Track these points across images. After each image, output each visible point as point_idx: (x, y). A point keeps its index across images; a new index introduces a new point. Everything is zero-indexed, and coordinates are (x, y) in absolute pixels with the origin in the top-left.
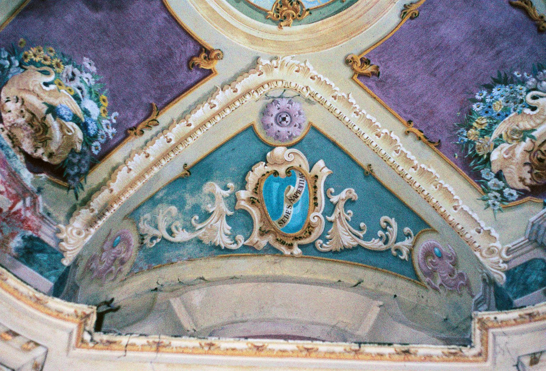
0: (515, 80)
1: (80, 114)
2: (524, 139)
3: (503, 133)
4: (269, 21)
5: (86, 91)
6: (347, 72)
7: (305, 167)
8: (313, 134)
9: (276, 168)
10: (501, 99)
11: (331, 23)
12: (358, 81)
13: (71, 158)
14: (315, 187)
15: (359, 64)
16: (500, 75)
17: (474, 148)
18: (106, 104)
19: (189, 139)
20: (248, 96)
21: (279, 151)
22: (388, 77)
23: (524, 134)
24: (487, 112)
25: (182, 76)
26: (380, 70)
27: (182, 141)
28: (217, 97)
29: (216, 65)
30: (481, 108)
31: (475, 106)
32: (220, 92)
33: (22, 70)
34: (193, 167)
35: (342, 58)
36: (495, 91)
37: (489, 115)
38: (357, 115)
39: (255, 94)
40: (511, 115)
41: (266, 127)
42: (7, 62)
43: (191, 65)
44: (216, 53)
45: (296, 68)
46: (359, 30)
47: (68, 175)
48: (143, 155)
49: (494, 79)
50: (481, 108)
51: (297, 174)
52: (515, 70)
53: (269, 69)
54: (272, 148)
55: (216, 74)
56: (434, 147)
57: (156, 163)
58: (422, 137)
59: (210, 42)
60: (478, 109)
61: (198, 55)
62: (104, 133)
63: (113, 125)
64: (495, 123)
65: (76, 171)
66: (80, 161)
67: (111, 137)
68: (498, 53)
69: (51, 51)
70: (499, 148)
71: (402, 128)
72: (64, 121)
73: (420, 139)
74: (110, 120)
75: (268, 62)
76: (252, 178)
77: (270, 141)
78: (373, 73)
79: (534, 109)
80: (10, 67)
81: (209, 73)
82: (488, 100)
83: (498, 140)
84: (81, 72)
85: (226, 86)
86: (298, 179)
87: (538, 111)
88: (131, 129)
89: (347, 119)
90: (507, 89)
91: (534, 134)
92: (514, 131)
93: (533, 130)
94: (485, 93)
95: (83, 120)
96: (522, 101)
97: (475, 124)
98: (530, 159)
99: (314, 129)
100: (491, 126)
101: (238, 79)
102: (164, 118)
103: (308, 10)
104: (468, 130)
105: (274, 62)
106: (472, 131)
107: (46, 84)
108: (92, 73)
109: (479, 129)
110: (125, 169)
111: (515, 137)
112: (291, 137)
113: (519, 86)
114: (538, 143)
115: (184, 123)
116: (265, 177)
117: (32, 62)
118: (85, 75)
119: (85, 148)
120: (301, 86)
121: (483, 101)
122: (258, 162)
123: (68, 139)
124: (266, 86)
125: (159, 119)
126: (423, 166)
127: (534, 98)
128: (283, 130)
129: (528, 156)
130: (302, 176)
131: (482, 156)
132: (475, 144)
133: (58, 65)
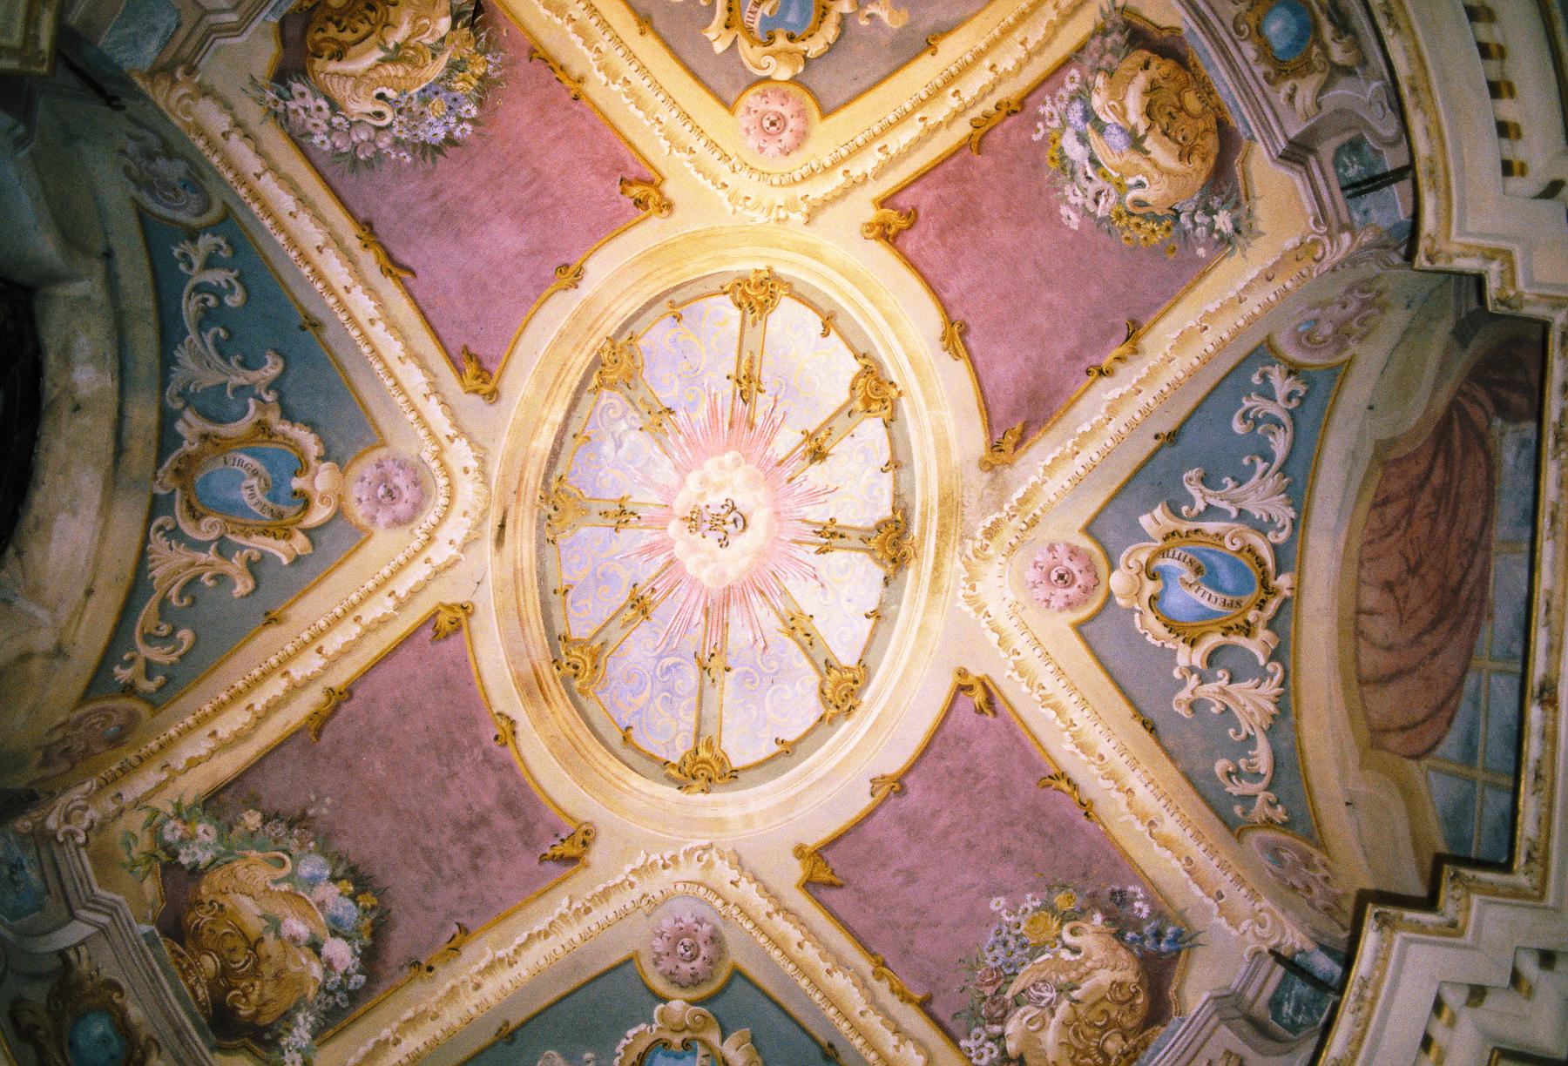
0: (410, 148)
1: (1093, 136)
2: (397, 47)
3: (430, 61)
4: (786, 280)
5: (1080, 175)
6: (670, 190)
7: (744, 44)
8: (731, 97)
9: (791, 46)
10: (432, 119)
11: (690, 270)
12: (653, 174)
13: (1116, 61)
14: (730, 10)
15: (650, 202)
16: (434, 160)
17: (477, 41)
18: (1050, 152)
19: (924, 96)
20: (828, 163)
21: (784, 73)
22: (606, 176)
23: (396, 56)
24: (455, 100)
25: (925, 199)
26: (619, 188)
27: (935, 93)
28: (875, 164)
29: (871, 214)
30: (464, 109)
31: (474, 113)
32: (869, 172)
33: (1177, 207)
34: (923, 51)
35: (678, 213)
36: (442, 135)
37: (453, 95)
38: (657, 119)
39: (815, 166)
40: (417, 90)
41: (801, 113)
42: (1197, 219)
43: (912, 216)
44: (872, 235)
45: (749, 203)
46: (648, 256)
47: (1122, 33)
48: (1000, 69)
49: (443, 154)
50: (464, 109)
51: (758, 34)
52: (409, 165)
53: (791, 206)
54: (794, 80)
55: (874, 201)
56: (541, 52)
57: (979, 55)
58: (557, 70)
59: (880, 250)
60: (468, 106)
61: (900, 231)
62: (1058, 105)
63: (1040, 118)
64: (442, 79)
65: (1109, 40)
66: (1101, 58)
67: (1047, 98)
68: (435, 195)
69: (1127, 238)
70: (437, 37)
71: (590, 89)
72: (1120, 124)
73: (562, 68)
74: (1045, 127)
75: (792, 216)
76: (829, 32)
77: (794, 90)
78: (630, 184)
79: (381, 96)
80: (1195, 212)
81: (884, 203)
82: (453, 120)
83: (439, 50)
84: (1084, 205)
85: (860, 180)
86: (756, 25)
87: (375, 93)
88: (1015, 112)
89: (674, 113)
90: (422, 136)
91: (381, 54)
92: (410, 61)
93: (383, 61)
94: (457, 133)
95: (1088, 126)
96: (400, 112)
97: (475, 82)
98: (388, 13)
99: (729, 106)
100: (449, 77)
101: (840, 191)
102: (962, 129)
103: (725, 293)
104: (486, 74)
105: (782, 214)
106: (480, 71)
107: (1140, 184)
108: (1068, 203)
109: (467, 73)
110: (1030, 45)
111: (412, 52)
112: (764, 95)
113: (403, 136)
114: (373, 38)
115: (930, 122)
116: (808, 33)
117: (1158, 220)
118: (1079, 200)
119: (1090, 79)
120: (744, 174)
121: (461, 120)
122: (818, 58)
123: (1117, 94)
124: (798, 178)
125: (969, 129)
126: (558, 21)
127: (380, 115)
128: (775, 106)
129: (392, 18)
130: (750, 31)
131: (464, 26)
132: (475, 47)
133: (1120, 216)
